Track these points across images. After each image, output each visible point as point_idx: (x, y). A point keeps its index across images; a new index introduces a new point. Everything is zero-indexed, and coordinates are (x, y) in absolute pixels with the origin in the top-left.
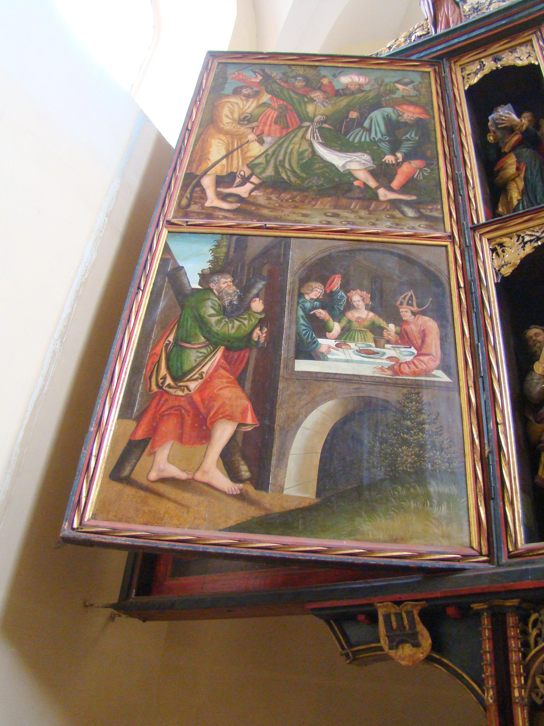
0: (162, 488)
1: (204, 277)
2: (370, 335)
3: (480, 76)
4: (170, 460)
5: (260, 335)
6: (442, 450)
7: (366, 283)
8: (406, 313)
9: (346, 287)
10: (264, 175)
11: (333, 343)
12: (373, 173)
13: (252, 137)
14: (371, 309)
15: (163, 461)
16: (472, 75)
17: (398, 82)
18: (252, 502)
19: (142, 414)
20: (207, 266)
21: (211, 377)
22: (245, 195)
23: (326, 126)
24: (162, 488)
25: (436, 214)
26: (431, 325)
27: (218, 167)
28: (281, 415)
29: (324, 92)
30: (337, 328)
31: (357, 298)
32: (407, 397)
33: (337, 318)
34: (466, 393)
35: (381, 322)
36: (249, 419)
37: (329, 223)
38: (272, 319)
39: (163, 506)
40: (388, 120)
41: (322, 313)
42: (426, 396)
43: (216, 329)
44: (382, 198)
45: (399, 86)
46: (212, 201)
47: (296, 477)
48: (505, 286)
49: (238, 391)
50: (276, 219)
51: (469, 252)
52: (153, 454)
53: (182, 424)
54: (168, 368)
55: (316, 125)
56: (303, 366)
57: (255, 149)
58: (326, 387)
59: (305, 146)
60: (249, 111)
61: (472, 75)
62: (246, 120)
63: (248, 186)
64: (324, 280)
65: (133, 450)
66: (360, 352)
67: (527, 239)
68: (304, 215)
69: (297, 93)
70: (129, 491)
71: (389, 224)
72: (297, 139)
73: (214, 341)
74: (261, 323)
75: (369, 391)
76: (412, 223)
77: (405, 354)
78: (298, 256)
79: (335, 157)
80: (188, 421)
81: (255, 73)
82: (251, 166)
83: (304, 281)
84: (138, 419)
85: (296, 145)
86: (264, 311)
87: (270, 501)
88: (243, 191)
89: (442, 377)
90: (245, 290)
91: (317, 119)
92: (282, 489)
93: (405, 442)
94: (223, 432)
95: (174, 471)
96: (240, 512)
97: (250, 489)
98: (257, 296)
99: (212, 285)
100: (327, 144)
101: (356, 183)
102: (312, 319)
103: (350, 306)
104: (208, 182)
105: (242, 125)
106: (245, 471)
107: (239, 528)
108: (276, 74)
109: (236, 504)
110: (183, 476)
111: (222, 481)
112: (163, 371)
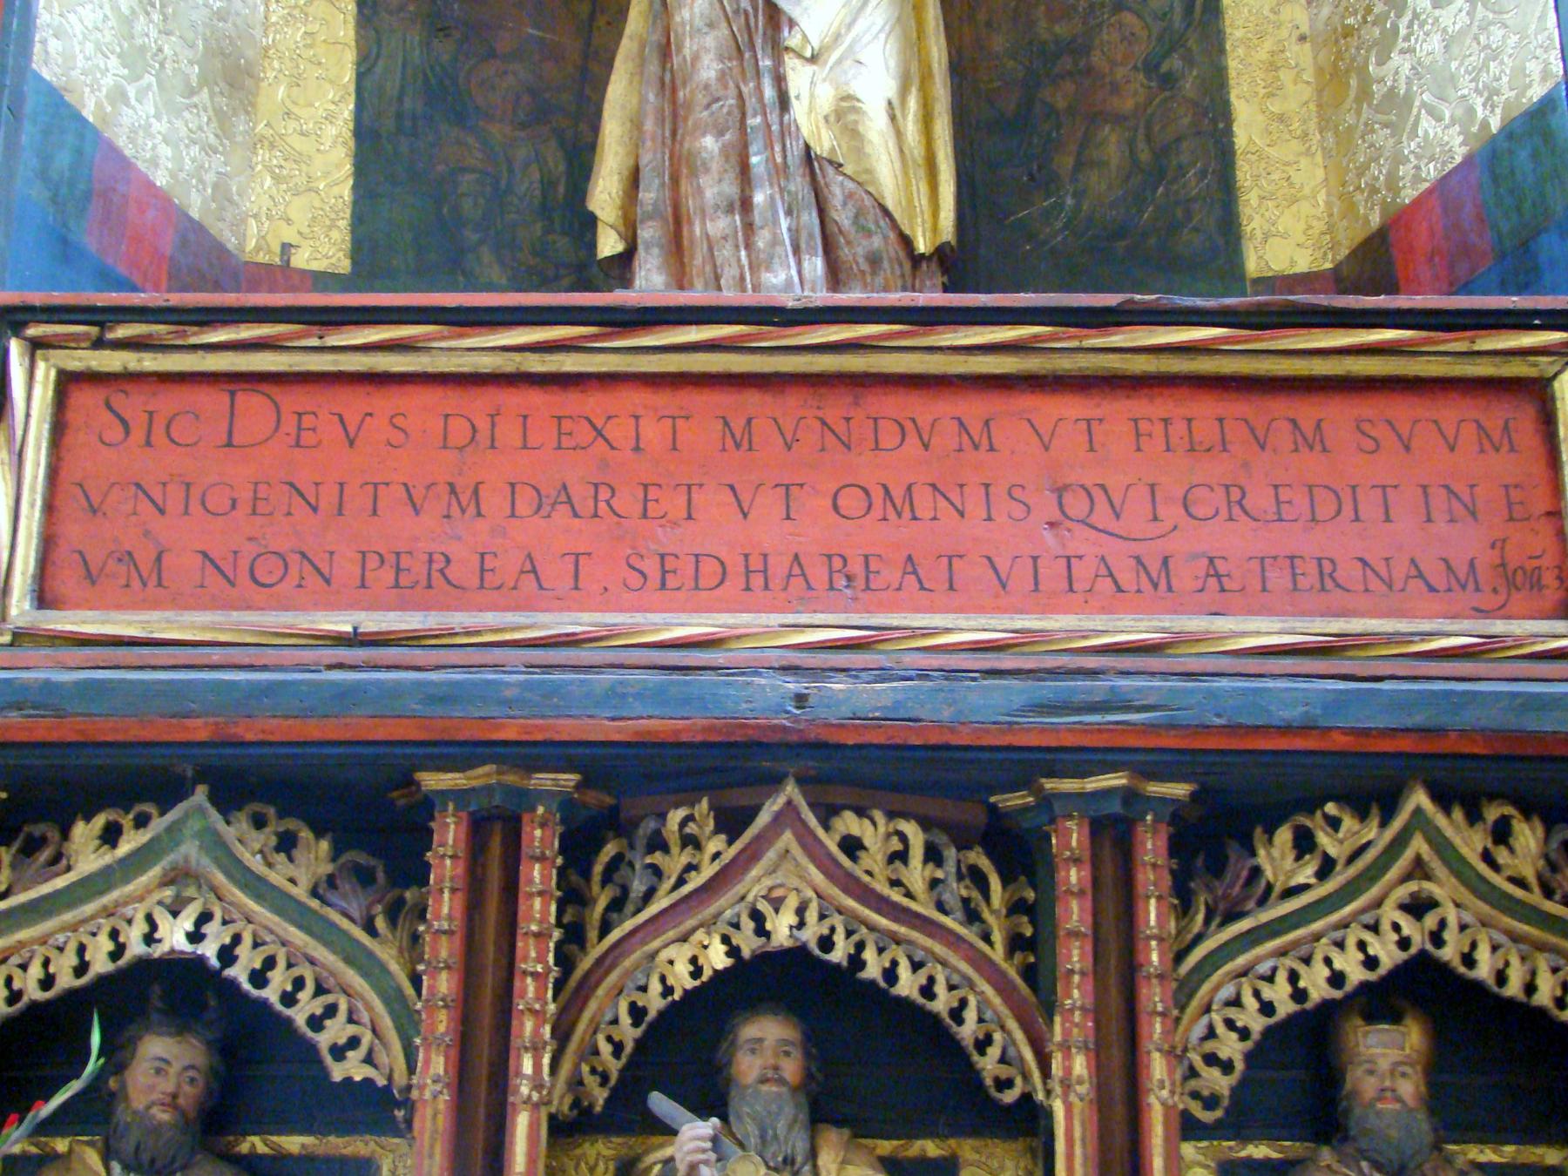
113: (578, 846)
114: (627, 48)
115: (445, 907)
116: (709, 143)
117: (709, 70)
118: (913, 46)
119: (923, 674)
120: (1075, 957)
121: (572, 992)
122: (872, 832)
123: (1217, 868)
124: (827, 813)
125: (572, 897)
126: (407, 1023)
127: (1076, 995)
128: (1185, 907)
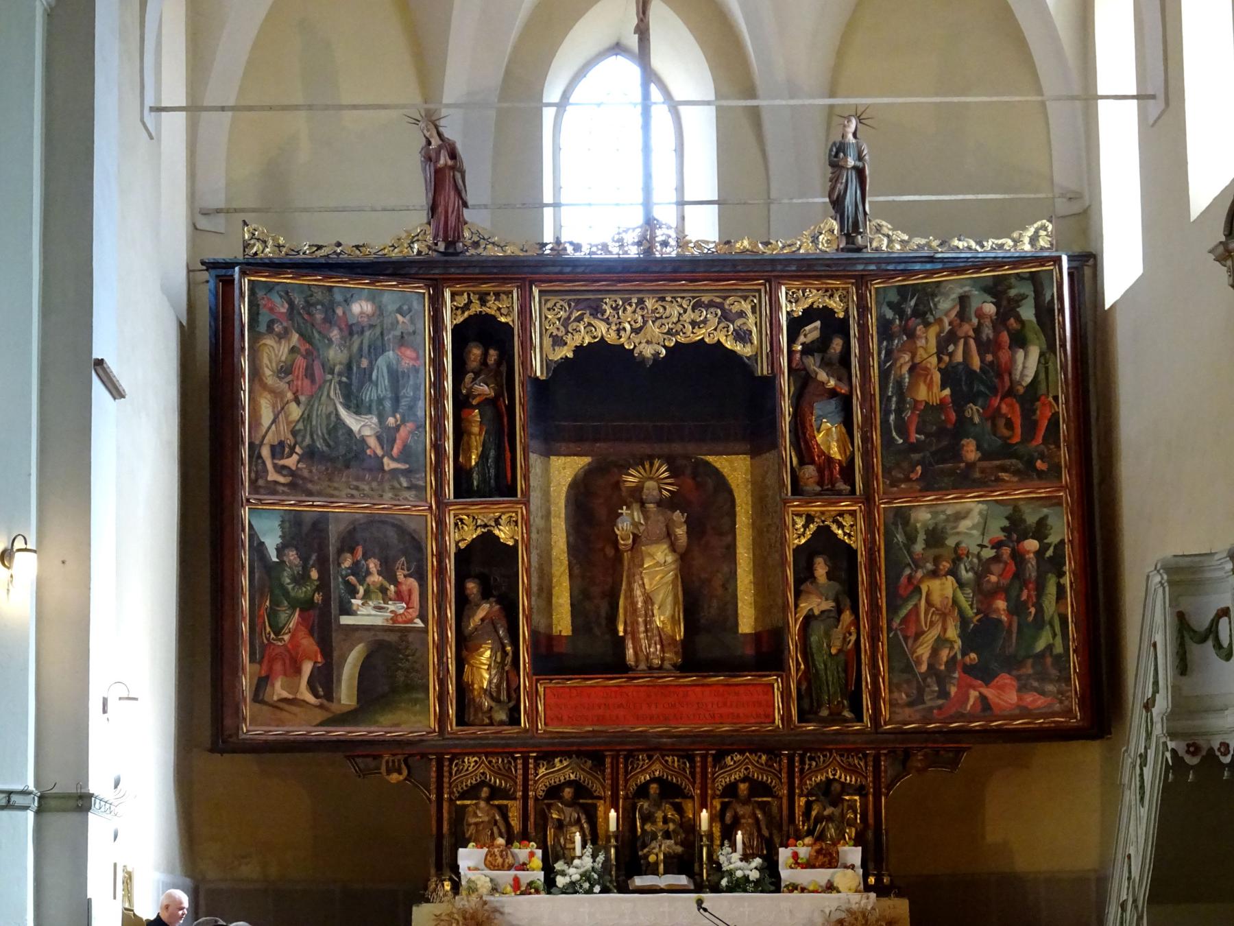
0: (281, 705)
1: (280, 550)
2: (380, 595)
3: (466, 314)
4: (283, 687)
5: (318, 597)
6: (417, 671)
7: (377, 551)
8: (401, 578)
9: (366, 556)
10: (305, 444)
11: (359, 602)
12: (379, 438)
13: (290, 395)
14: (379, 573)
15: (279, 690)
16: (459, 312)
17: (400, 311)
18: (327, 709)
19: (262, 658)
20: (279, 541)
21: (296, 629)
22: (294, 468)
23: (344, 379)
24: (281, 705)
25: (421, 483)
26: (413, 583)
27: (270, 433)
28: (336, 654)
29: (341, 330)
30: (361, 590)
31: (373, 565)
32: (400, 638)
33: (361, 582)
34: (433, 635)
35: (386, 584)
36: (319, 659)
37: (352, 496)
38: (324, 585)
39: (285, 715)
40: (389, 367)
41: (352, 579)
42: (411, 637)
43: (293, 594)
44: (386, 468)
45: (400, 318)
46: (272, 476)
47: (346, 695)
48: (460, 554)
49: (311, 640)
50: (319, 494)
51: (441, 523)
52: (273, 685)
53: (284, 664)
54: (270, 626)
55: (336, 379)
56: (345, 620)
57: (295, 412)
58: (358, 634)
59: (331, 409)
60: (283, 358)
61: (459, 312)
62: (285, 371)
63: (295, 457)
64: (352, 551)
65: (262, 683)
66: (375, 608)
67: (479, 522)
68: (336, 489)
69: (320, 333)
70: (265, 708)
71: (390, 495)
72: (324, 398)
73: (294, 604)
74: (318, 589)
75: (382, 636)
76: (407, 494)
77: (400, 608)
78: (334, 532)
79: (353, 421)
80: (287, 662)
81: (281, 297)
82: (294, 433)
83: (340, 552)
84: (261, 663)
85: (325, 409)
86: (319, 579)
87: (334, 707)
88: (291, 462)
89: (419, 623)
90: (305, 559)
91: (337, 369)
92: (339, 700)
93: (401, 669)
94: (307, 668)
95: (285, 694)
96: (321, 716)
97: (325, 702)
98: (313, 566)
99: (285, 559)
100: (347, 407)
101: (368, 452)
102: (347, 583)
103: (368, 573)
104: (265, 452)
105: (281, 379)
106: (321, 693)
107: (322, 724)
108: (298, 300)
109: (318, 711)
110: (290, 696)
111: (310, 698)
112: (268, 629)
113: (626, 758)
114: (623, 593)
115: (608, 771)
116: (640, 620)
117: (640, 605)
118: (676, 596)
119: (674, 737)
120: (698, 776)
121: (626, 781)
122: (670, 759)
123: (720, 762)
124: (663, 757)
125: (626, 767)
126: (604, 787)
127: (698, 781)
128: (714, 766)
